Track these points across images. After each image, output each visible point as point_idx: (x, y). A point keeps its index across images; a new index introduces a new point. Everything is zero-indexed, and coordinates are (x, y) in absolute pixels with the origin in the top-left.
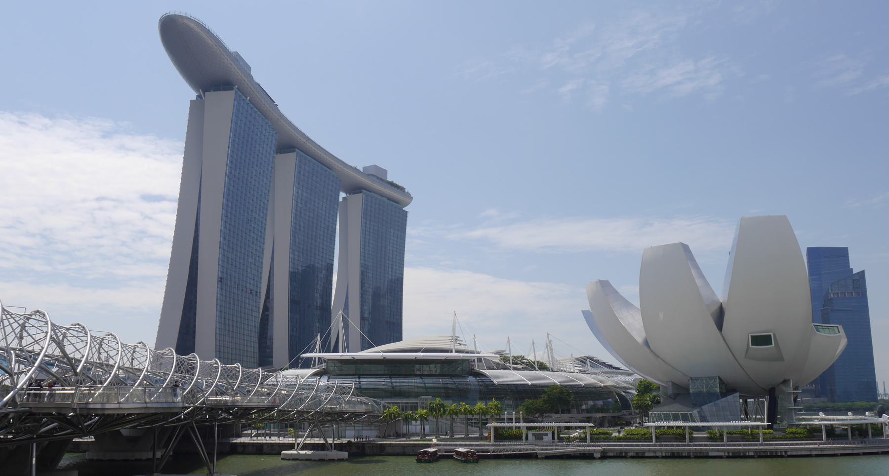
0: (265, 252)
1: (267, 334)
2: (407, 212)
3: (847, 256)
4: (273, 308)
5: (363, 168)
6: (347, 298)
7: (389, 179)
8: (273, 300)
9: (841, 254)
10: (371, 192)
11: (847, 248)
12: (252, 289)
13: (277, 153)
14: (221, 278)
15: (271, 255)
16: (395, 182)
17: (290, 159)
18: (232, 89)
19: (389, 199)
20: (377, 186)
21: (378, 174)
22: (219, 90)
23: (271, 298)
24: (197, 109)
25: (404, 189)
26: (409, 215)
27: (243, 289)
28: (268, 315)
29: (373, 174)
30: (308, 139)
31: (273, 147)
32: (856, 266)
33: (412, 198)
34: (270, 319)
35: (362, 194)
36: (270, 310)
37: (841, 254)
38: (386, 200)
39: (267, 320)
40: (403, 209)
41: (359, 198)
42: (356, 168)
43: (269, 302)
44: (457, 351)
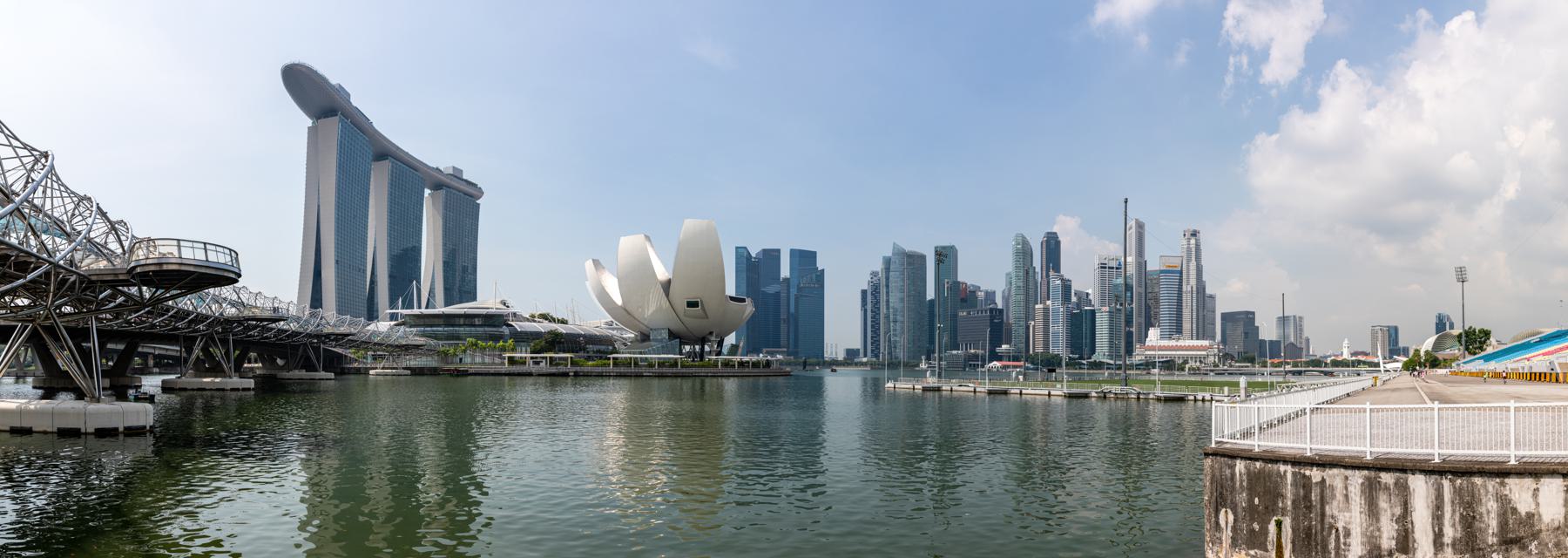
0: (369, 240)
2: (479, 204)
3: (815, 257)
7: (464, 177)
9: (812, 256)
10: (449, 188)
11: (815, 253)
17: (386, 165)
18: (337, 115)
19: (465, 194)
20: (455, 183)
21: (457, 174)
24: (312, 132)
26: (481, 207)
29: (452, 173)
30: (398, 148)
31: (371, 158)
32: (820, 265)
37: (812, 256)
38: (462, 195)
41: (442, 193)
42: (437, 169)
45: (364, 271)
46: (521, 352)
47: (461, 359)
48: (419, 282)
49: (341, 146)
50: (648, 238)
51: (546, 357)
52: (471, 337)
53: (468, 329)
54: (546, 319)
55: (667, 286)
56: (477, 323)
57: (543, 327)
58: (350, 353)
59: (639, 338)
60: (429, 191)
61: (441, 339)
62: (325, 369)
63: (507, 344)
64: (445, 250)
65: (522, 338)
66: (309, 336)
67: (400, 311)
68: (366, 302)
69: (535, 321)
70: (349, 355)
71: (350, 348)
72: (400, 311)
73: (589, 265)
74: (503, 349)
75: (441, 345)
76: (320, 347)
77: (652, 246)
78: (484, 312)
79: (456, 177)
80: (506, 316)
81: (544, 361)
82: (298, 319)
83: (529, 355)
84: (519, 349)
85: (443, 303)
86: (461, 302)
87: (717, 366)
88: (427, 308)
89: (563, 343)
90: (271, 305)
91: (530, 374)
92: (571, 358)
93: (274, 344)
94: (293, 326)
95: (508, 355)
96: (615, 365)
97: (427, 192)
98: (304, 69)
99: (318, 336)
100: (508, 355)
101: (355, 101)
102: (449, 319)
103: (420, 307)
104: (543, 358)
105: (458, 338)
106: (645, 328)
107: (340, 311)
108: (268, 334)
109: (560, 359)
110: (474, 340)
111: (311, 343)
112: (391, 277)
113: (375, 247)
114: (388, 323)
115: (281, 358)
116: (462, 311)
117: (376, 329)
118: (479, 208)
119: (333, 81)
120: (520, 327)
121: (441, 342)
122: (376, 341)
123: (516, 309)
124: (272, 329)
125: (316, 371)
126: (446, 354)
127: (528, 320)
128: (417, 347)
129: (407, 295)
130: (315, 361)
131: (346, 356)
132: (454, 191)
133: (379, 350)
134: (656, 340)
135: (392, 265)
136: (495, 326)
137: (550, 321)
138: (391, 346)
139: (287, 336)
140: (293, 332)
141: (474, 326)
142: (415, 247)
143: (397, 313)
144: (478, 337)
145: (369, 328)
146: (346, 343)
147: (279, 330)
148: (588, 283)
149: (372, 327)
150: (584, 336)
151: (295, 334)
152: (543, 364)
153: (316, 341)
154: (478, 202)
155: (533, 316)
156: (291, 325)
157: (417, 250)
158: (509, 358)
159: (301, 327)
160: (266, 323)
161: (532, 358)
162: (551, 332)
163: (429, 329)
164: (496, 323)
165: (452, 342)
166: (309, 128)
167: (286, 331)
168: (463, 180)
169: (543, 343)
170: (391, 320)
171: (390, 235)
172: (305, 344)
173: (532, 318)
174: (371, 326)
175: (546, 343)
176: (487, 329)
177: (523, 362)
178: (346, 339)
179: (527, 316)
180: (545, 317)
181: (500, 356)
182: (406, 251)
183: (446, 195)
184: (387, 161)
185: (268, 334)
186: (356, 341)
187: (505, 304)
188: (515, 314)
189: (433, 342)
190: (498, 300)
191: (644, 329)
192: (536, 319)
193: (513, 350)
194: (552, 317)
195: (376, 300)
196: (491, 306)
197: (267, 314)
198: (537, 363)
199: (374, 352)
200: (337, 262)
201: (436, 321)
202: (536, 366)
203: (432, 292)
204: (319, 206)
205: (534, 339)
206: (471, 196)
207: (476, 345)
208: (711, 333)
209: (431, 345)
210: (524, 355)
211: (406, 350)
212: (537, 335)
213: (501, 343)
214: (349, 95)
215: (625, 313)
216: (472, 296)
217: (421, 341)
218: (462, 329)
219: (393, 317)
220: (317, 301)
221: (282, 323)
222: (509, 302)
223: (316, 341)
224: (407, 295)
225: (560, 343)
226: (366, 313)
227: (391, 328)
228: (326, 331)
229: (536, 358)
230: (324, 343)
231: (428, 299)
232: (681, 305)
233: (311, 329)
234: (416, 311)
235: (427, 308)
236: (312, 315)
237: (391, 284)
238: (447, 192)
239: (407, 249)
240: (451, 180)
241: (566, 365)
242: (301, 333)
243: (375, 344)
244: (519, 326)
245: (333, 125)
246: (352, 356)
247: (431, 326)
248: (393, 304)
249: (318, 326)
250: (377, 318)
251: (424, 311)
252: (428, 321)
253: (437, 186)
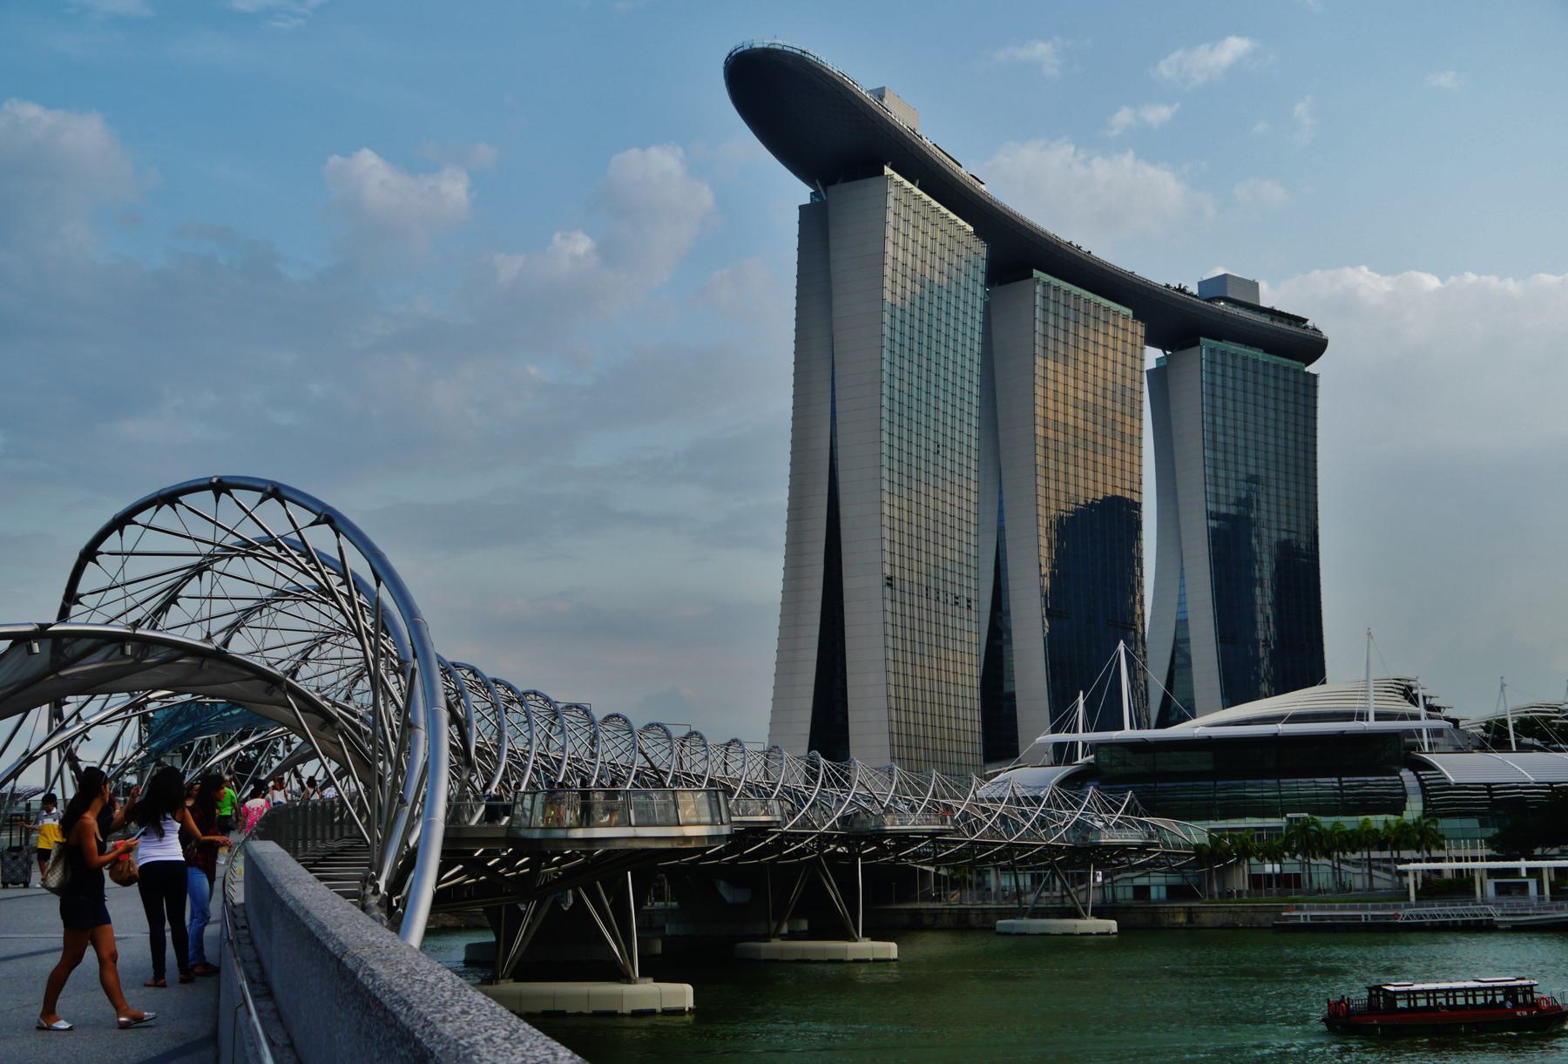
1: (1001, 687)
2: (1315, 377)
4: (1009, 632)
5: (1200, 284)
8: (1008, 613)
12: (957, 594)
14: (890, 578)
15: (995, 518)
23: (1004, 609)
25: (1305, 320)
26: (1321, 383)
27: (938, 598)
28: (1001, 648)
34: (1005, 654)
35: (1198, 347)
36: (1005, 636)
39: (1001, 657)
40: (1307, 369)
43: (1001, 618)
44: (1380, 716)
62: (874, 933)
72: (1081, 737)
91: (1483, 927)
118: (1315, 387)
125: (850, 937)
130: (841, 908)
143: (1073, 745)
154: (1311, 369)
161: (1492, 873)
166: (801, 207)
170: (1057, 763)
173: (1495, 737)
177: (1462, 885)
196: (1356, 706)
216: (1312, 673)
219: (1063, 753)
238: (1212, 351)
244: (1460, 768)
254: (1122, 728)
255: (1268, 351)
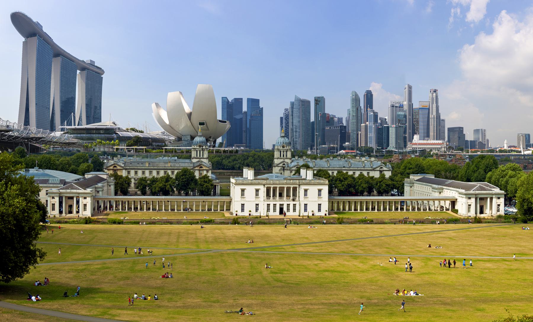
6: (81, 110)
7: (95, 65)
9: (257, 101)
11: (259, 100)
13: (54, 57)
16: (98, 66)
17: (59, 59)
19: (96, 72)
20: (91, 68)
21: (92, 63)
22: (32, 37)
24: (25, 44)
26: (103, 78)
30: (65, 51)
33: (104, 72)
37: (257, 101)
38: (94, 73)
41: (85, 72)
45: (49, 108)
46: (122, 146)
47: (94, 149)
48: (74, 114)
49: (38, 50)
50: (181, 93)
51: (134, 148)
52: (99, 139)
53: (97, 135)
54: (134, 131)
55: (190, 115)
56: (101, 133)
57: (132, 134)
58: (43, 146)
59: (177, 139)
60: (79, 71)
61: (85, 140)
63: (116, 142)
64: (86, 99)
65: (122, 139)
66: (23, 138)
67: (65, 127)
68: (50, 122)
69: (128, 132)
70: (42, 147)
71: (42, 144)
72: (65, 127)
73: (154, 106)
74: (114, 145)
75: (85, 143)
76: (28, 143)
77: (183, 97)
78: (105, 127)
79: (91, 65)
80: (115, 129)
81: (133, 150)
82: (18, 131)
83: (125, 147)
84: (121, 145)
85: (86, 123)
86: (94, 123)
87: (213, 152)
88: (78, 125)
89: (141, 142)
90: (6, 124)
92: (145, 148)
93: (7, 142)
94: (16, 134)
95: (116, 147)
96: (166, 152)
97: (78, 72)
98: (21, 15)
99: (27, 139)
100: (116, 147)
101: (45, 30)
102: (88, 131)
103: (75, 125)
104: (132, 149)
105: (93, 139)
106: (179, 135)
107: (38, 127)
108: (4, 138)
109: (140, 149)
110: (100, 140)
111: (24, 142)
112: (62, 111)
113: (54, 97)
114: (60, 132)
115: (10, 149)
116: (94, 127)
117: (54, 135)
119: (35, 20)
120: (122, 134)
121: (84, 141)
122: (54, 141)
123: (120, 125)
124: (6, 135)
126: (87, 147)
127: (125, 131)
128: (74, 143)
129: (69, 119)
131: (40, 148)
132: (91, 71)
133: (55, 145)
134: (185, 140)
135: (62, 106)
136: (110, 134)
137: (135, 132)
138: (62, 143)
139: (13, 139)
140: (16, 137)
141: (100, 134)
142: (72, 97)
143: (64, 128)
144: (102, 139)
145: (51, 135)
146: (41, 142)
147: (9, 136)
148: (153, 114)
149: (53, 134)
150: (151, 138)
151: (17, 137)
152: (132, 152)
153: (26, 141)
155: (127, 129)
156: (15, 133)
157: (74, 99)
158: (116, 148)
159: (20, 134)
160: (3, 132)
161: (127, 149)
162: (135, 137)
163: (79, 135)
164: (111, 133)
165: (90, 141)
167: (13, 136)
168: (95, 66)
169: (132, 142)
170: (62, 131)
171: (61, 92)
172: (21, 142)
174: (52, 134)
175: (134, 142)
176: (106, 135)
178: (41, 140)
179: (125, 129)
180: (133, 130)
181: (112, 148)
182: (68, 99)
183: (87, 73)
184: (60, 57)
185: (4, 138)
186: (45, 141)
187: (114, 124)
188: (119, 128)
189: (81, 141)
190: (111, 122)
191: (179, 135)
192: (129, 131)
193: (118, 145)
194: (136, 130)
195: (54, 122)
196: (108, 125)
197: (4, 128)
198: (129, 151)
199: (54, 146)
200: (36, 104)
201: (82, 131)
202: (129, 153)
203: (80, 118)
204: (28, 78)
205: (128, 140)
206: (99, 73)
207: (101, 143)
208: (210, 137)
209: (80, 143)
210: (123, 147)
211: (69, 145)
212: (129, 138)
213: (113, 142)
214: (42, 27)
215: (171, 128)
216: (100, 121)
217: (75, 141)
218: (94, 135)
219: (62, 130)
220: (27, 122)
221: (11, 132)
222: (116, 123)
223: (26, 141)
224: (69, 119)
225: (140, 142)
226: (50, 128)
227: (62, 135)
228: (31, 136)
229: (129, 149)
230: (30, 142)
231: (79, 121)
232: (196, 124)
233: (24, 135)
234: (73, 127)
235: (78, 125)
236: (25, 129)
237: (61, 114)
238: (87, 71)
239: (69, 98)
240: (90, 66)
241: (143, 152)
242: (20, 137)
243: (54, 142)
244: (121, 134)
245: (35, 41)
246: (43, 148)
247: (80, 134)
248: (62, 124)
249: (28, 134)
250: (55, 130)
251: (77, 127)
252: (78, 131)
253: (83, 69)
254: (72, 126)
255: (96, 73)
